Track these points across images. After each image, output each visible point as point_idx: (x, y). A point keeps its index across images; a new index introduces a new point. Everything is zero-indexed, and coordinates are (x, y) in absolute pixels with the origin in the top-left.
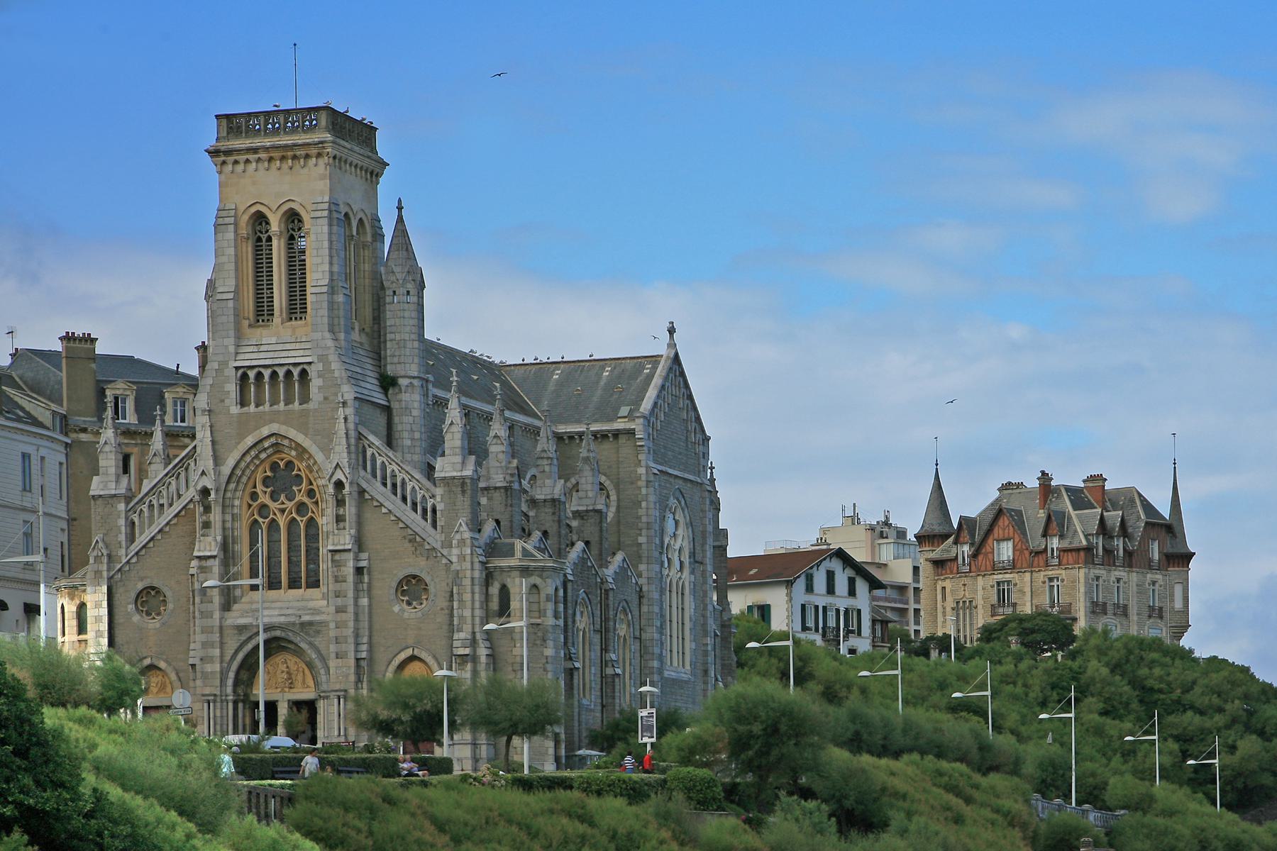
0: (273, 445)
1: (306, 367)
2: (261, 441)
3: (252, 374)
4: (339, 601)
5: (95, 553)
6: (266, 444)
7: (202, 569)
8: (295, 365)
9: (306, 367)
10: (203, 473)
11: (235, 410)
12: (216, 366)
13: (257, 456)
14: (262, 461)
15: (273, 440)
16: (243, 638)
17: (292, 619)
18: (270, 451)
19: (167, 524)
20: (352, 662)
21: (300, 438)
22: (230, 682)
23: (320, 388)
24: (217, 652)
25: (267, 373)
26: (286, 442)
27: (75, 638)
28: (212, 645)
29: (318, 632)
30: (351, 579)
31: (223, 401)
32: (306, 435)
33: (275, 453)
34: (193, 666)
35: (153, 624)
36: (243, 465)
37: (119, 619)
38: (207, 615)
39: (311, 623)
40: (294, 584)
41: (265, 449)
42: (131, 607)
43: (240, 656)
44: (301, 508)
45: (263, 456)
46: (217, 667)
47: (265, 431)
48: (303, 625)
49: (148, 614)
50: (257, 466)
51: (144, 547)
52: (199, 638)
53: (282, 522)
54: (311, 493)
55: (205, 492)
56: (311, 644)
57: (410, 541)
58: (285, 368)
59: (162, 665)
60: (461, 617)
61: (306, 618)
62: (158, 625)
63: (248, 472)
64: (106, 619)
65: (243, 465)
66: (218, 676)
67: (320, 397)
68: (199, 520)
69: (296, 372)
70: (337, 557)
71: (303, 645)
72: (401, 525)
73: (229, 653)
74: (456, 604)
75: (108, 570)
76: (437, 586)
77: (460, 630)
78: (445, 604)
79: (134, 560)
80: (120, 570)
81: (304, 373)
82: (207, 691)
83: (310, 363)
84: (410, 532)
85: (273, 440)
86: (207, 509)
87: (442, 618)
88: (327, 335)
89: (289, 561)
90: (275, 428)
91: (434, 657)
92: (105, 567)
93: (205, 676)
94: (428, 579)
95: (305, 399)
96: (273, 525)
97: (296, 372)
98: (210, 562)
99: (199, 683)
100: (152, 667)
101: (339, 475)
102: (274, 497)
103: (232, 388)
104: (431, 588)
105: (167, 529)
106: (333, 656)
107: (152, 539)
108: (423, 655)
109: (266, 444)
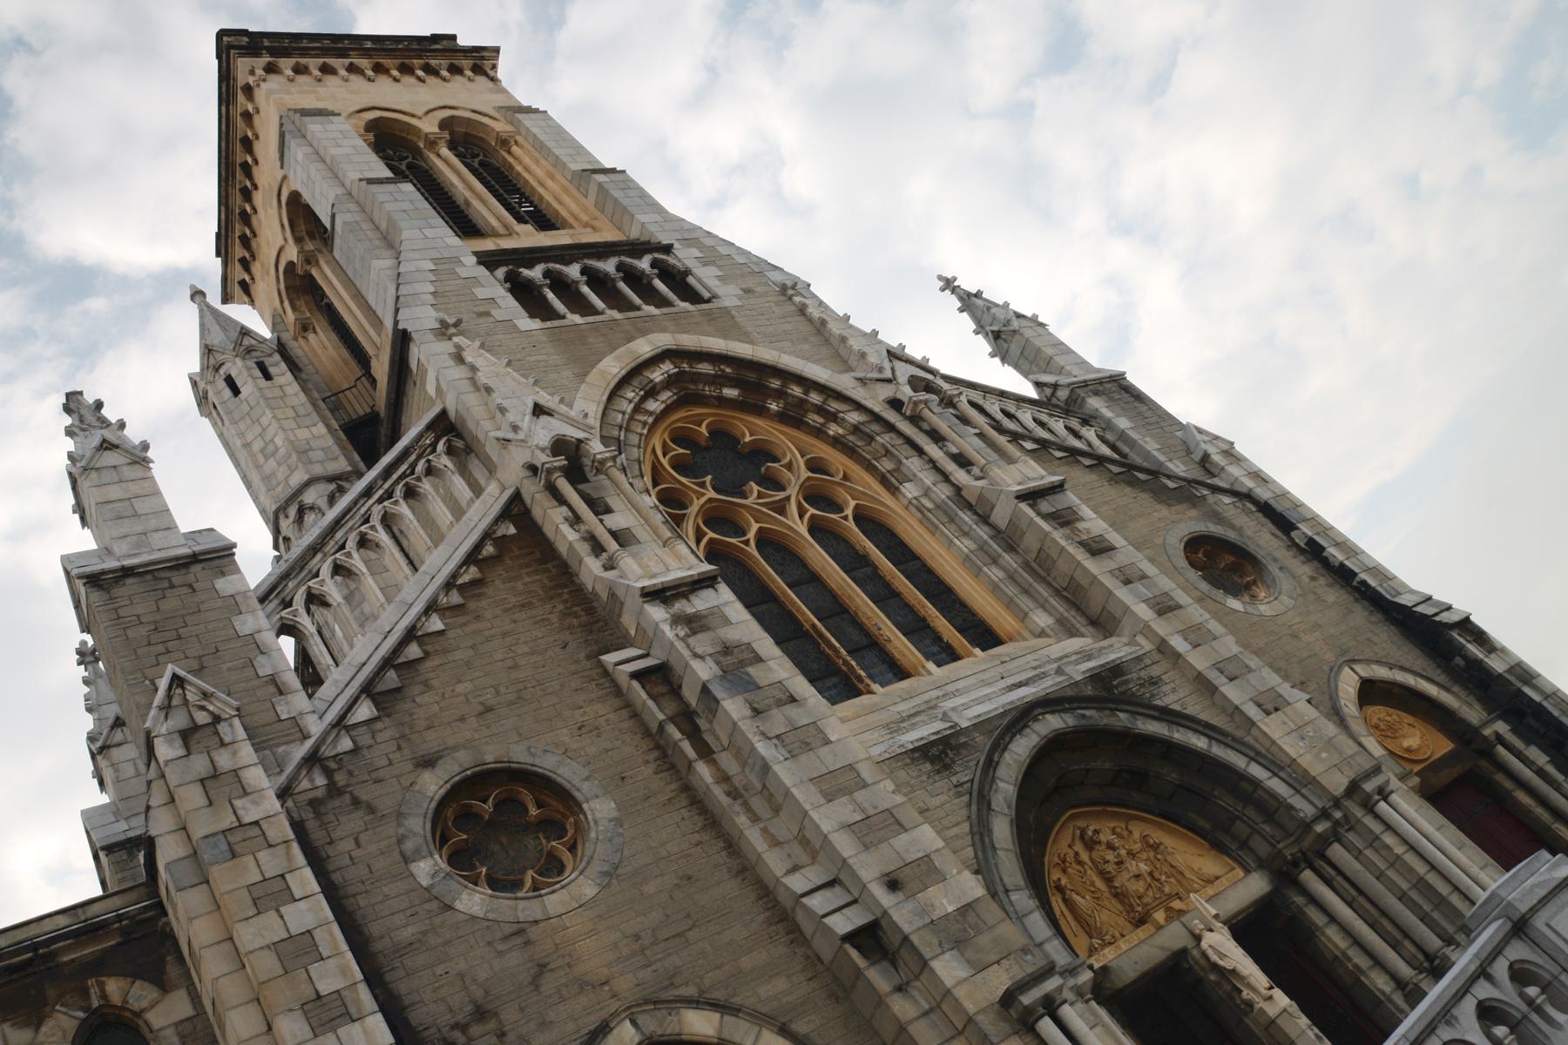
5: (179, 720)
6: (657, 375)
15: (667, 367)
16: (964, 773)
18: (666, 396)
26: (705, 368)
28: (893, 823)
32: (751, 342)
34: (873, 938)
37: (392, 925)
38: (803, 741)
42: (427, 868)
43: (1002, 830)
45: (654, 406)
47: (644, 347)
64: (332, 938)
82: (999, 980)
87: (1333, 595)
90: (664, 340)
91: (1402, 668)
92: (247, 753)
96: (775, 546)
99: (948, 969)
107: (410, 635)
108: (1381, 673)
109: (657, 375)
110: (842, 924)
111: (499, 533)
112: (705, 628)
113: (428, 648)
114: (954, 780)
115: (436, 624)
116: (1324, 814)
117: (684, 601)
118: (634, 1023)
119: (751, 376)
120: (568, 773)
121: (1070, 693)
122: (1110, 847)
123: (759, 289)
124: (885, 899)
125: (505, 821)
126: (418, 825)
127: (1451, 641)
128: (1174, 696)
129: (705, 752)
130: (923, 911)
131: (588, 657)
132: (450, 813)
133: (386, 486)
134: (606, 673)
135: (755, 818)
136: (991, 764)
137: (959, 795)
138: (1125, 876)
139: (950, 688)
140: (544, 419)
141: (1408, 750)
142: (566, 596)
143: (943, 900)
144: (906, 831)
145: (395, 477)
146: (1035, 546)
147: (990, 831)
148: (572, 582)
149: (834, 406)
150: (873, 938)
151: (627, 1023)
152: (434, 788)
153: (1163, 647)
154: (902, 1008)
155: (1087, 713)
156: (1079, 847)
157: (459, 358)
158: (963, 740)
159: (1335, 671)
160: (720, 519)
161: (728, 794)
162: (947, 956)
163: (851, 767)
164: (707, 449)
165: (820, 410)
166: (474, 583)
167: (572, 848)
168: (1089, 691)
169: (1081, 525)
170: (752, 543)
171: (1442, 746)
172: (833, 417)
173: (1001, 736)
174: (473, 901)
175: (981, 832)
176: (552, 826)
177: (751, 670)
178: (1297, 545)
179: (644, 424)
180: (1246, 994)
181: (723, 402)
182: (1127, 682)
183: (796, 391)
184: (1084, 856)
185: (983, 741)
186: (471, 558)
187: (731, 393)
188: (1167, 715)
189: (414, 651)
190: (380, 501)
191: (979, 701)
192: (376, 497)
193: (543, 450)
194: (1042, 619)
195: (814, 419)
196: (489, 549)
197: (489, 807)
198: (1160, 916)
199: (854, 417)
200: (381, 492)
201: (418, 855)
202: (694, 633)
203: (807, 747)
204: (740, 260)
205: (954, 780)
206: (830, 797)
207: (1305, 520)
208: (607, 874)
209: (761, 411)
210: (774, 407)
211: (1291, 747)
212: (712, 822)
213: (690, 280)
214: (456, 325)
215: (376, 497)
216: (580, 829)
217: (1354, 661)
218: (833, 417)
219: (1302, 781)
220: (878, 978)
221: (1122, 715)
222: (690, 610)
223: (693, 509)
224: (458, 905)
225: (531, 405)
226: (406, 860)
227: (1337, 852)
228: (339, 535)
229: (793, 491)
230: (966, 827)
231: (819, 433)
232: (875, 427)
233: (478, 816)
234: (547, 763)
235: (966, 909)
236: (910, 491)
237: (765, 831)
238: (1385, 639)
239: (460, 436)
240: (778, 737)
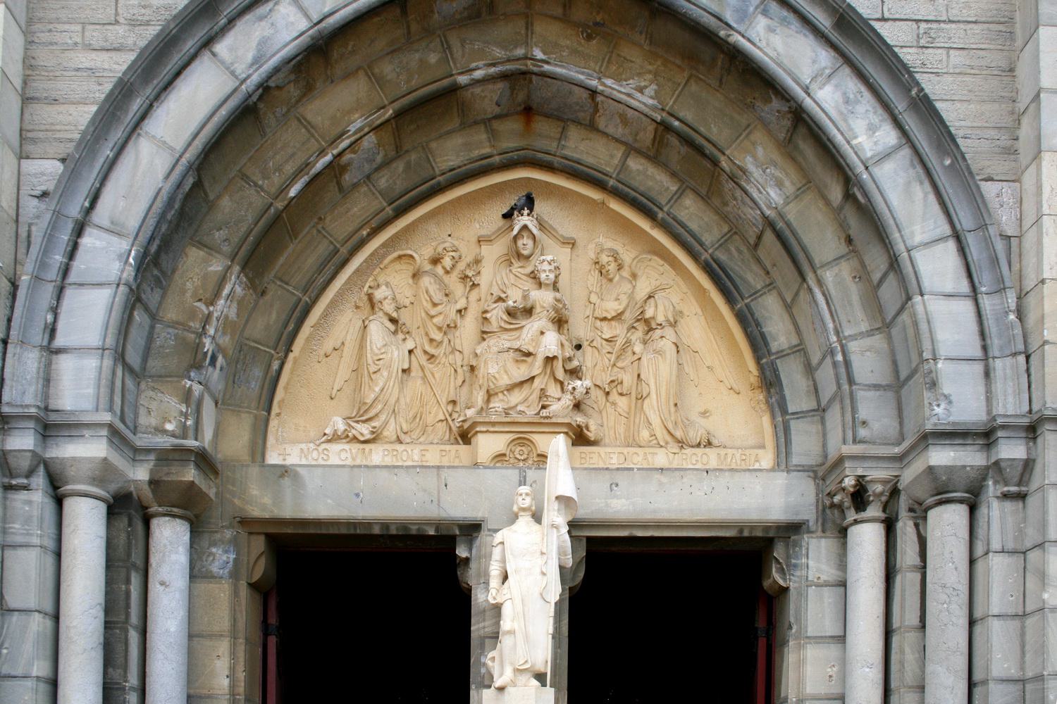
138: (505, 341)
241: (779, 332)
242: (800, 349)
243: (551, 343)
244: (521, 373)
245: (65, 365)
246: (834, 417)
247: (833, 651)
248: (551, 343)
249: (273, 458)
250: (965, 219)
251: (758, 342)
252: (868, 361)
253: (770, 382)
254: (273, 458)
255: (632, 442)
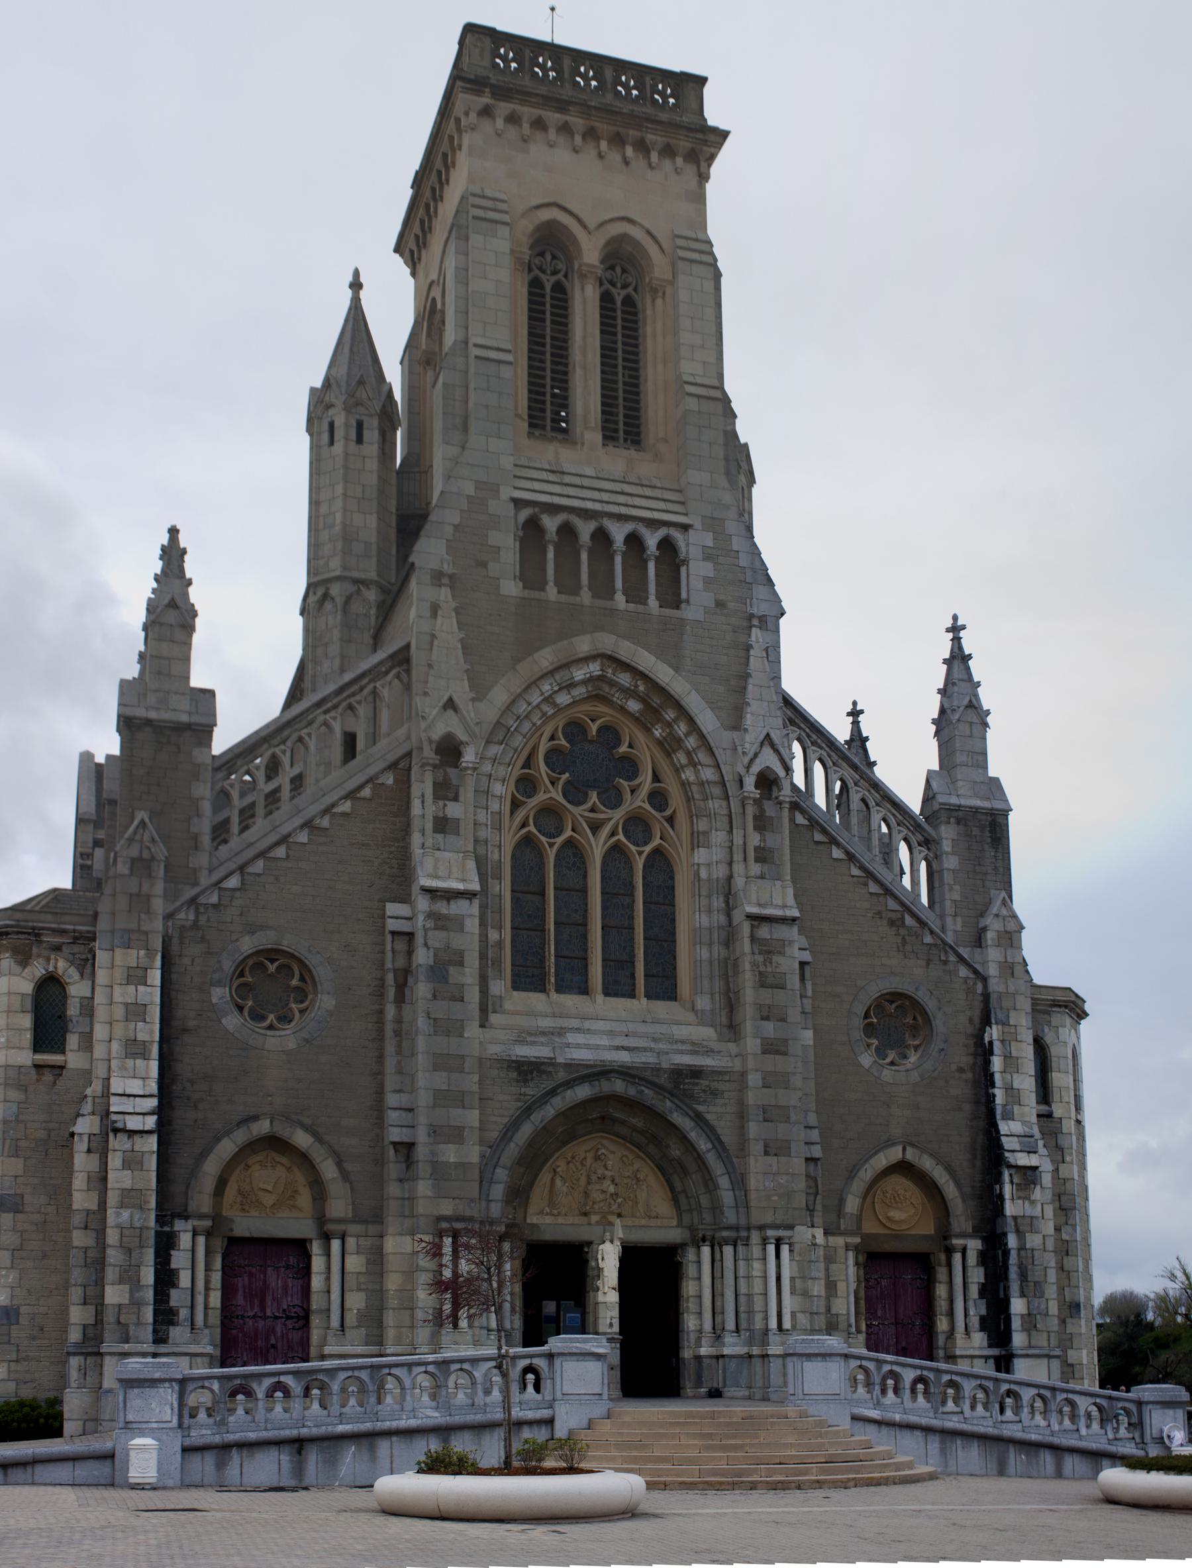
0: (591, 680)
1: (676, 534)
2: (566, 666)
3: (551, 524)
4: (769, 1029)
6: (579, 674)
7: (440, 922)
8: (653, 524)
9: (676, 534)
10: (450, 704)
11: (511, 588)
12: (470, 489)
13: (549, 700)
14: (559, 710)
15: (594, 668)
16: (533, 1090)
17: (650, 1059)
19: (327, 811)
20: (797, 1164)
21: (663, 674)
22: (498, 1191)
23: (707, 581)
24: (472, 1117)
25: (585, 530)
26: (625, 679)
27: (26, 1057)
28: (458, 1099)
29: (714, 1093)
30: (794, 981)
31: (483, 565)
32: (677, 669)
33: (591, 698)
34: (406, 1149)
35: (285, 1039)
36: (522, 708)
39: (696, 1073)
40: (618, 985)
41: (572, 685)
44: (637, 826)
45: (563, 699)
46: (474, 1153)
47: (583, 645)
48: (679, 1074)
49: (257, 1017)
50: (547, 719)
51: (262, 854)
52: (426, 1081)
53: (597, 848)
54: (658, 798)
55: (450, 751)
56: (699, 1119)
57: (892, 923)
58: (629, 527)
59: (302, 1139)
60: (1009, 1089)
61: (687, 1060)
62: (292, 1045)
63: (526, 727)
65: (522, 708)
66: (476, 1175)
67: (708, 599)
68: (423, 807)
69: (652, 541)
70: (764, 932)
71: (678, 1119)
72: (873, 888)
73: (500, 1121)
74: (997, 1063)
75: (167, 896)
76: (950, 1019)
77: (1009, 1116)
78: (965, 1060)
79: (233, 882)
80: (193, 901)
81: (666, 544)
82: (447, 1208)
83: (685, 528)
84: (892, 905)
85: (594, 668)
86: (445, 791)
88: (723, 481)
89: (584, 938)
91: (949, 1169)
93: (439, 1171)
94: (930, 1005)
95: (672, 597)
96: (573, 854)
97: (652, 541)
98: (460, 907)
99: (424, 1188)
100: (275, 1144)
101: (767, 759)
102: (575, 793)
103: (506, 542)
104: (939, 1024)
105: (325, 822)
106: (756, 1148)
108: (927, 1164)
109: (579, 674)
110: (395, 1134)
111: (380, 781)
112: (443, 928)
113: (291, 853)
114: (523, 1090)
115: (303, 837)
116: (737, 1228)
117: (445, 903)
118: (271, 1122)
119: (656, 700)
120: (322, 973)
121: (647, 1074)
122: (605, 1167)
123: (731, 605)
124: (422, 1136)
125: (272, 982)
126: (228, 966)
127: (1000, 1174)
128: (718, 1113)
129: (400, 999)
130: (433, 1153)
131: (380, 900)
132: (251, 962)
133: (335, 701)
134: (383, 916)
135: (399, 1051)
136: (553, 1092)
137: (519, 1100)
139: (587, 1024)
140: (450, 712)
141: (889, 1218)
142: (393, 849)
143: (450, 1154)
144: (464, 1107)
145: (345, 694)
146: (738, 954)
147: (517, 1129)
148: (404, 839)
149: (702, 756)
150: (406, 1149)
151: (268, 1121)
152: (246, 948)
153: (743, 1074)
154: (393, 1189)
155: (647, 1091)
156: (590, 1155)
157: (435, 609)
158: (550, 1069)
159: (890, 1143)
160: (550, 816)
161: (395, 1031)
162: (430, 1182)
163: (463, 1057)
164: (591, 742)
165: (688, 753)
166: (344, 815)
167: (302, 1012)
168: (663, 1080)
169: (775, 958)
170: (556, 847)
171: (928, 1228)
172: (694, 764)
173: (574, 1080)
174: (231, 1021)
175: (514, 1125)
176: (301, 994)
177: (452, 970)
178: (982, 1038)
179: (544, 714)
180: (599, 1283)
181: (623, 709)
182: (697, 1084)
183: (681, 728)
184: (589, 1162)
185: (562, 1075)
186: (351, 795)
187: (634, 706)
188: (699, 1119)
189: (281, 852)
190: (326, 712)
191: (588, 1047)
192: (324, 708)
193: (430, 741)
194: (703, 1003)
195: (682, 758)
196: (367, 792)
197: (272, 968)
198: (594, 1218)
199: (708, 774)
200: (329, 705)
201: (219, 984)
202: (435, 929)
203: (448, 1033)
204: (743, 561)
205: (523, 1090)
206: (436, 1068)
207: (1005, 1024)
208: (307, 1041)
209: (648, 730)
210: (657, 733)
211: (753, 1183)
212: (380, 1038)
213: (683, 570)
214: (451, 577)
215: (324, 708)
216: (313, 1002)
217: (912, 1145)
218: (694, 764)
219: (742, 1202)
220: (393, 1168)
221: (668, 1103)
222: (444, 911)
223: (533, 802)
224: (224, 1021)
225: (445, 698)
226: (212, 984)
227: (728, 1250)
228: (286, 733)
229: (618, 815)
230: (505, 1120)
231: (677, 770)
232: (717, 790)
233: (266, 968)
234: (312, 960)
235: (462, 1166)
236: (701, 856)
237: (399, 1062)
238: (960, 1142)
239: (408, 671)
240: (435, 1019)
241: (678, 1186)
242: (684, 1191)
243: (612, 1189)
244: (602, 1196)
245: (493, 1205)
246: (695, 1213)
247: (696, 1282)
248: (612, 1189)
249: (528, 1221)
250: (731, 1170)
251: (672, 1189)
252: (705, 1201)
253: (675, 1200)
254: (528, 1221)
255: (633, 1216)
